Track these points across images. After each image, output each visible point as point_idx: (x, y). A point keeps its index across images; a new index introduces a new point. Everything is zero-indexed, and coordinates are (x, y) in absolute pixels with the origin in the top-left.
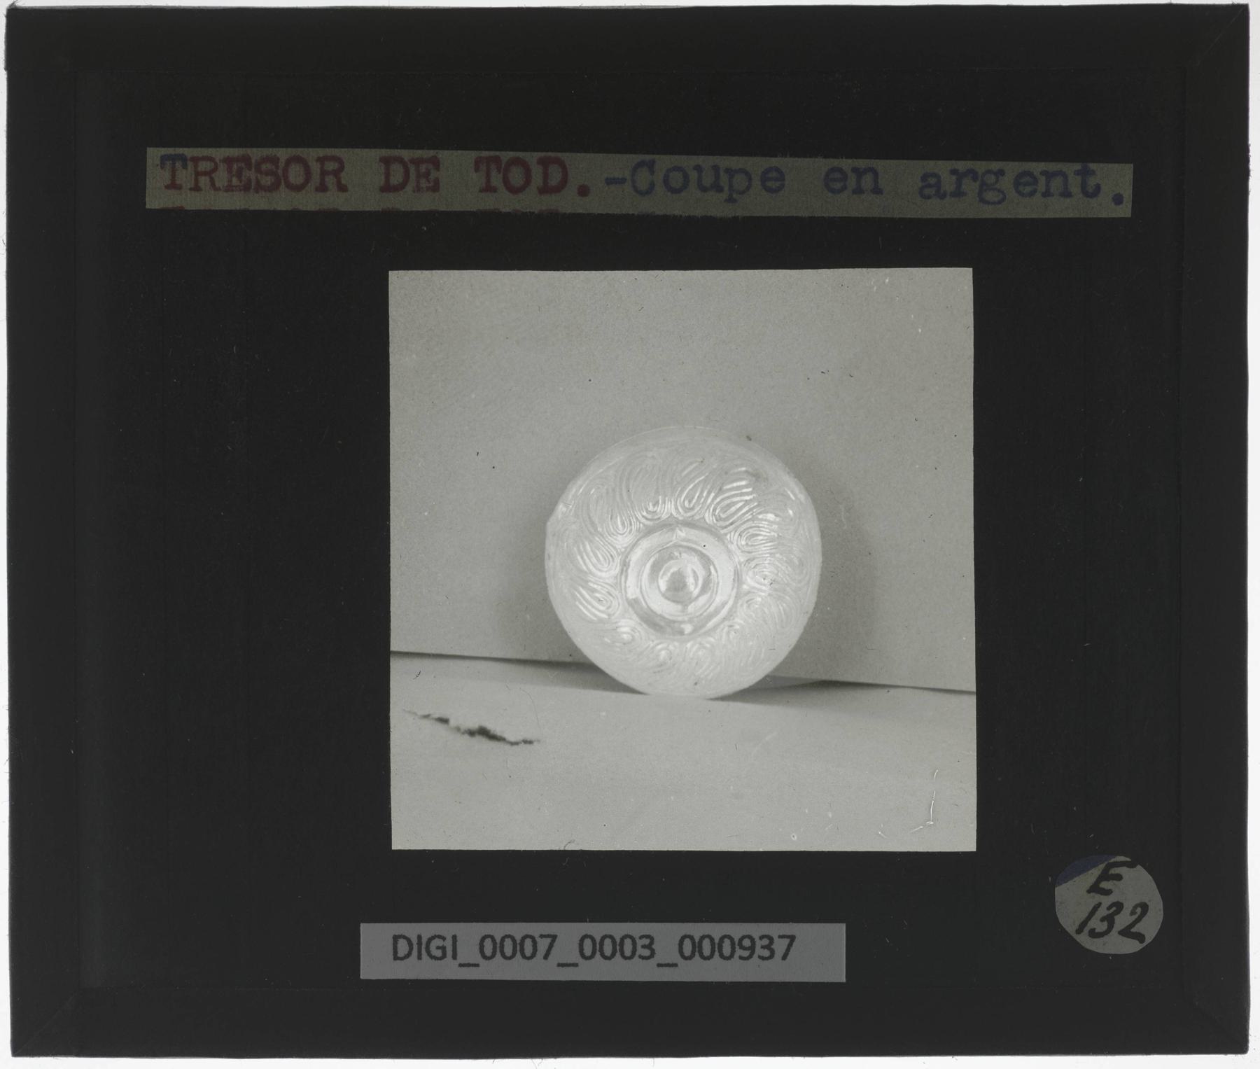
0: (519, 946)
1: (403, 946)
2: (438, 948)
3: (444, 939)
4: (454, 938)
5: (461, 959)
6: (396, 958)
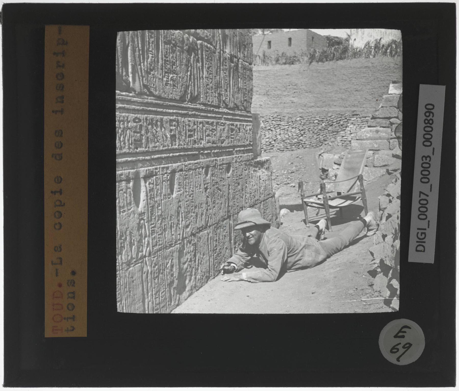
0: (423, 206)
1: (419, 248)
2: (421, 235)
3: (418, 233)
4: (418, 229)
5: (426, 227)
6: (424, 251)
